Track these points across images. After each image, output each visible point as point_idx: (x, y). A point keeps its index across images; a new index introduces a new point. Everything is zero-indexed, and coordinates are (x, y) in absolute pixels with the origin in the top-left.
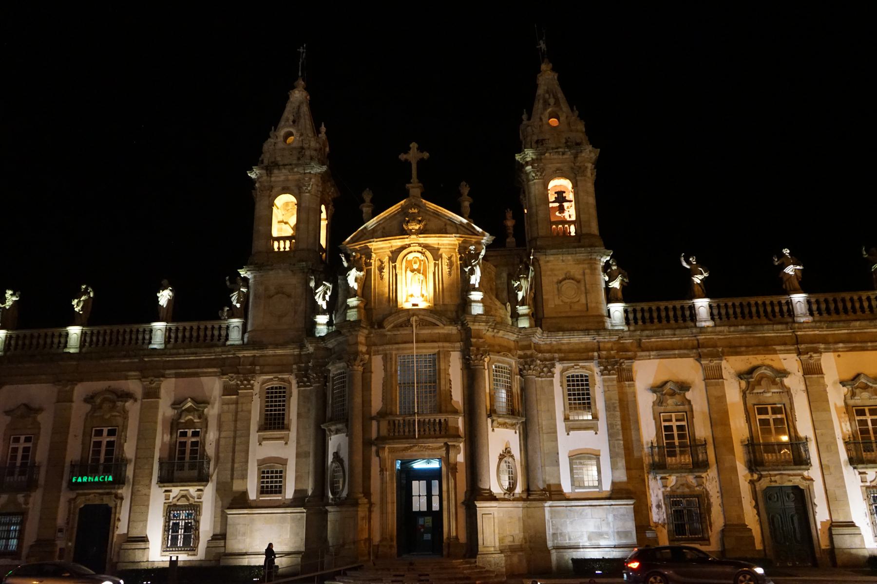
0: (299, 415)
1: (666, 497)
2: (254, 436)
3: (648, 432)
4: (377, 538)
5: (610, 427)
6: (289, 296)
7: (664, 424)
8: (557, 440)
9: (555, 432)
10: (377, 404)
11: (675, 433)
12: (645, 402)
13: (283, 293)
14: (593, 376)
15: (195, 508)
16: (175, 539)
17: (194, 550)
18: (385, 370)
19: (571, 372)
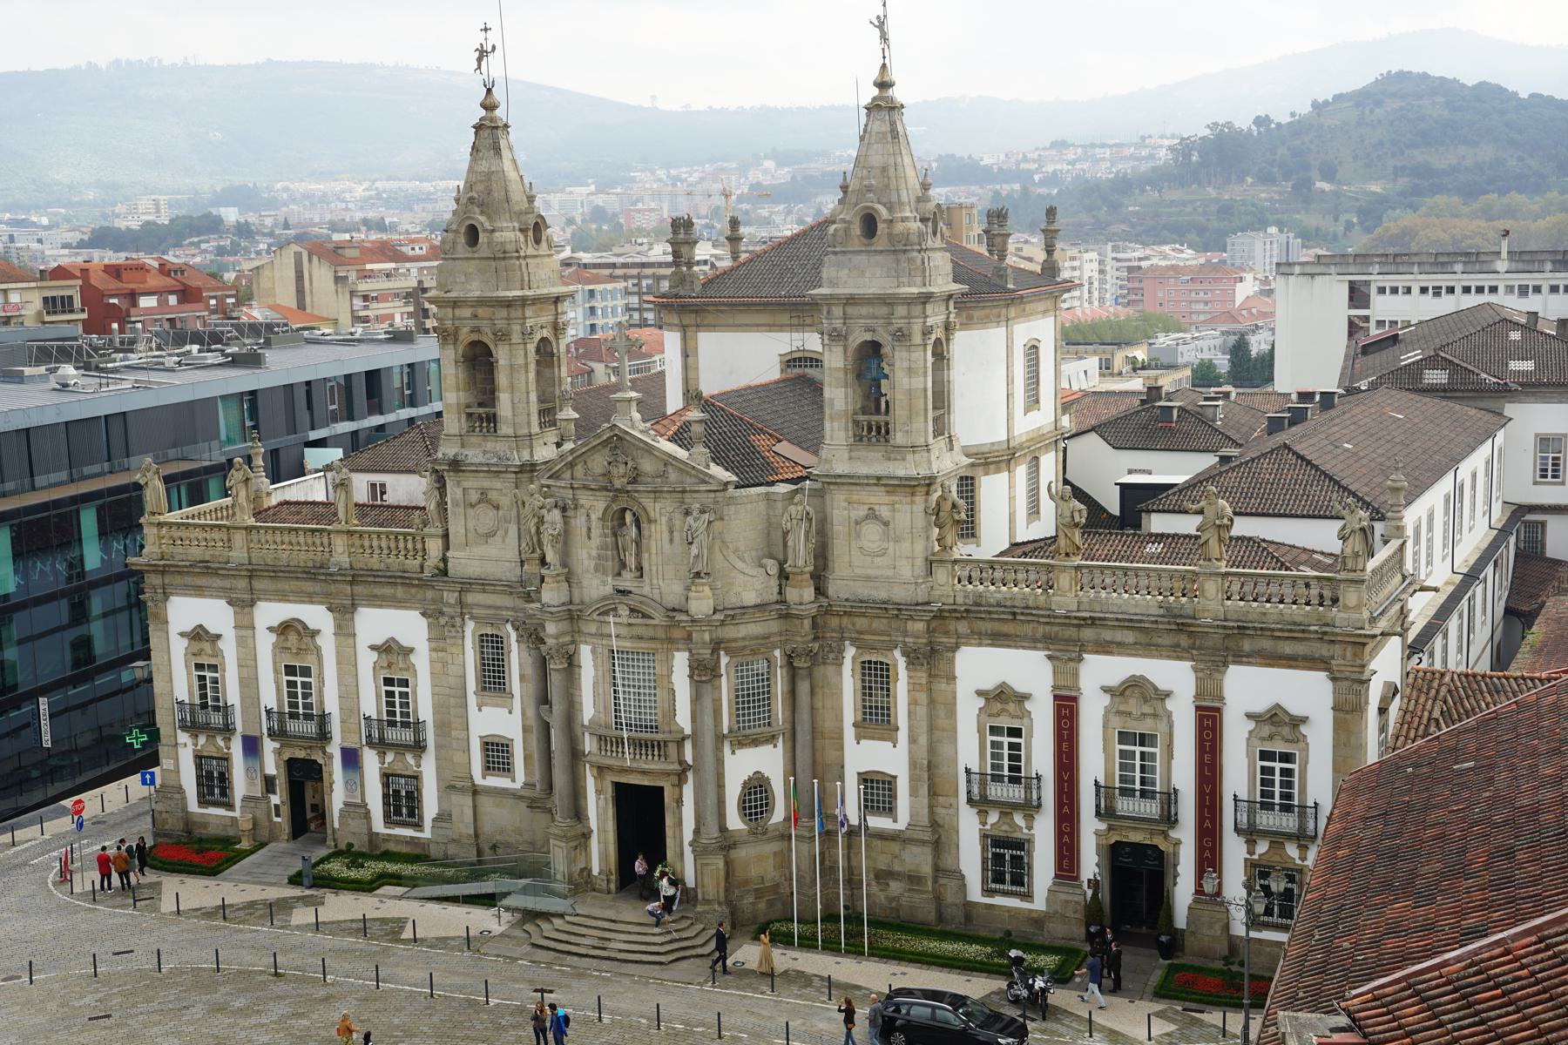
0: (522, 677)
1: (984, 836)
2: (472, 700)
3: (968, 751)
4: (595, 872)
5: (912, 740)
6: (497, 508)
7: (990, 738)
8: (841, 748)
9: (841, 738)
10: (588, 712)
11: (1006, 752)
12: (968, 711)
13: (488, 502)
14: (896, 666)
15: (416, 777)
16: (398, 812)
17: (418, 826)
18: (596, 667)
19: (867, 658)
